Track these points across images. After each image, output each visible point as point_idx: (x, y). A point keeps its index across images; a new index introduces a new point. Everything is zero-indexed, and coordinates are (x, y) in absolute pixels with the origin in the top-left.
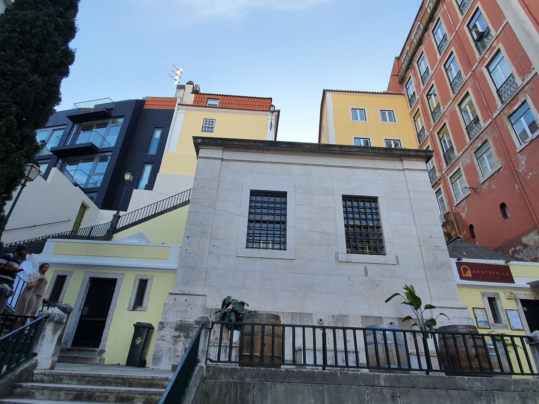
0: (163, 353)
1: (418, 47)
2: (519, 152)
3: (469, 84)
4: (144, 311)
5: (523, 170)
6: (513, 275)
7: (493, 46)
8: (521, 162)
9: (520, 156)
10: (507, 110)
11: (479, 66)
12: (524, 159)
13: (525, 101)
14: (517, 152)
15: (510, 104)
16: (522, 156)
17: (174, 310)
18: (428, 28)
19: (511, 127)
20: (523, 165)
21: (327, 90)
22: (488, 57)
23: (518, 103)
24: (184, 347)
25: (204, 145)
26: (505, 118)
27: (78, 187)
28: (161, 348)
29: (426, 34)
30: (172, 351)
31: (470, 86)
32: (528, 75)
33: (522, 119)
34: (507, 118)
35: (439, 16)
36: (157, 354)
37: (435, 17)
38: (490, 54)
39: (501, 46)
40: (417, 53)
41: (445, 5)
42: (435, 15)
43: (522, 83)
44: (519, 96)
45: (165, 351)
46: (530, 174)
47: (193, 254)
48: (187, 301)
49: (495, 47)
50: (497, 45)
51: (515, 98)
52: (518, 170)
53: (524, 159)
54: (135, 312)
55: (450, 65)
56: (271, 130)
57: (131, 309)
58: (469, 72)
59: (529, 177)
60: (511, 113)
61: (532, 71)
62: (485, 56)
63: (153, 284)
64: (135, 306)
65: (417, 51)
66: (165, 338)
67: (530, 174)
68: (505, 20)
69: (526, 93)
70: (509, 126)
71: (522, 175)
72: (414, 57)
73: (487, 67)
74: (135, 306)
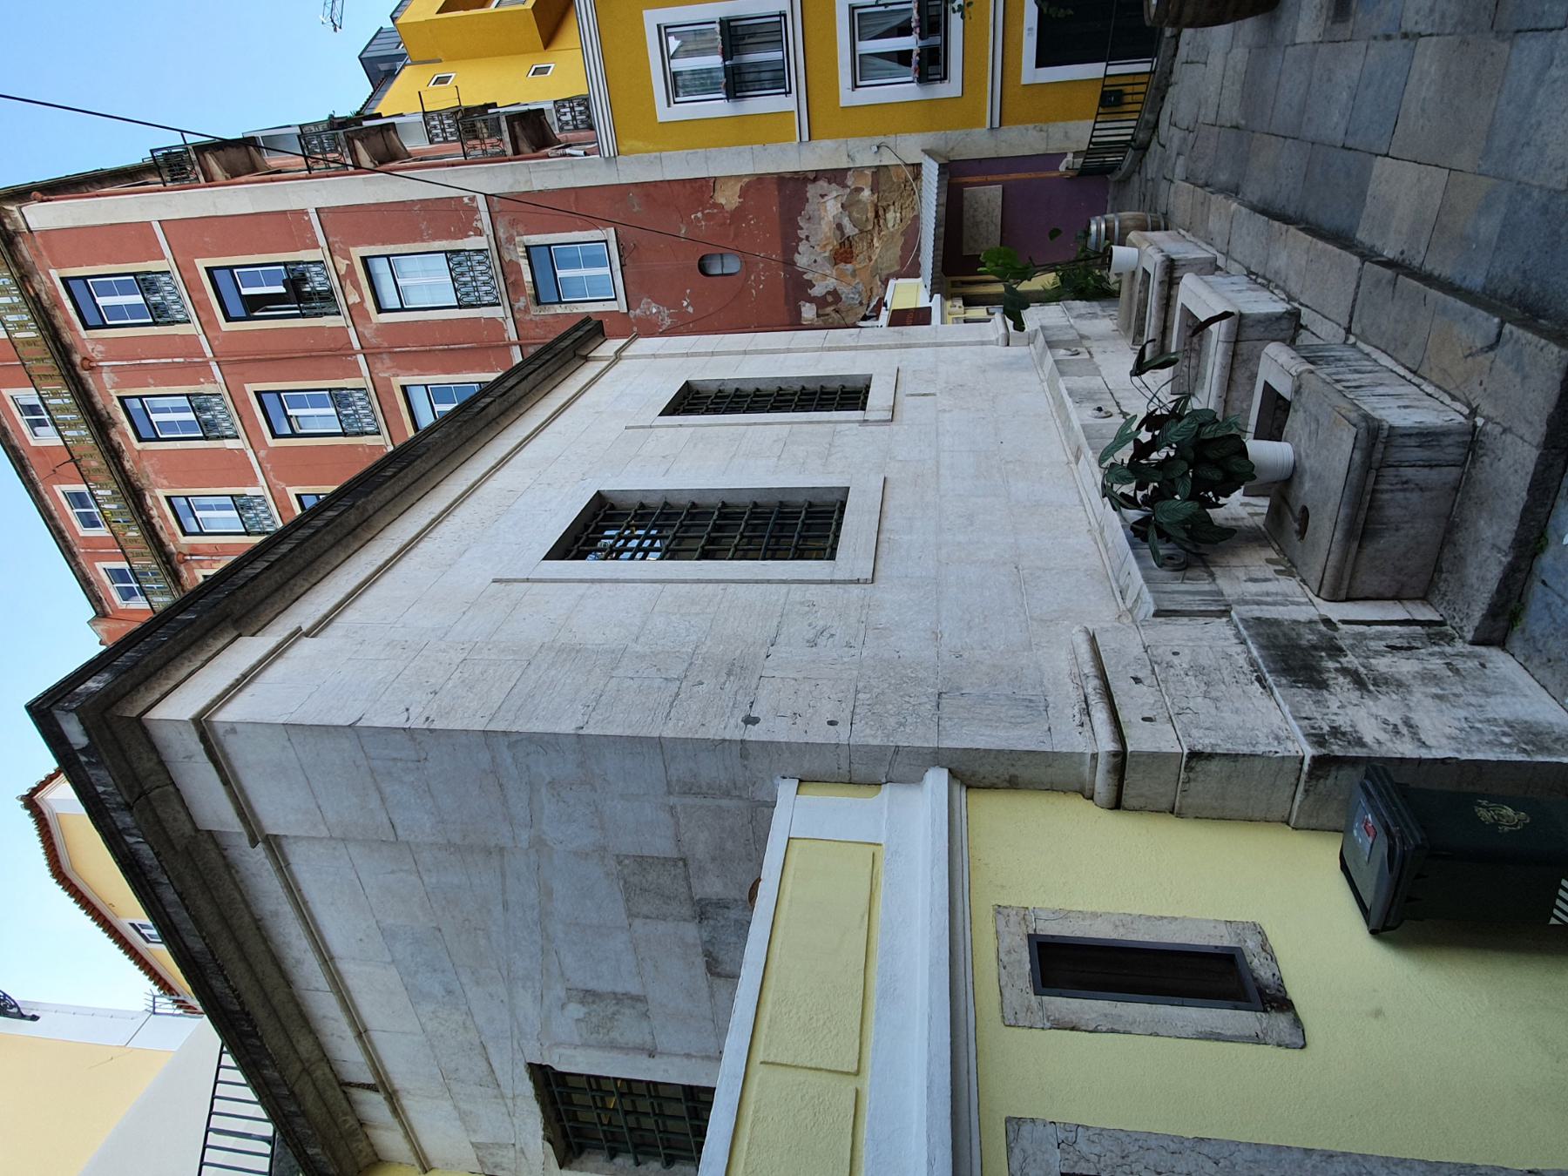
0: (1480, 722)
1: (142, 506)
2: (628, 310)
3: (386, 375)
4: (1261, 933)
5: (670, 316)
6: (913, 306)
7: (342, 272)
8: (651, 313)
9: (638, 311)
10: (518, 301)
11: (360, 329)
12: (648, 303)
13: (528, 248)
14: (626, 311)
15: (513, 286)
16: (639, 307)
17: (1213, 711)
18: (117, 446)
19: (563, 306)
20: (659, 312)
21: (35, 791)
22: (361, 296)
23: (522, 266)
24: (1386, 652)
25: (135, 687)
26: (535, 311)
27: (372, 90)
28: (1461, 730)
29: (125, 463)
30: (1443, 689)
31: (394, 376)
32: (477, 217)
33: (560, 274)
34: (538, 308)
35: (114, 393)
36: (1506, 740)
37: (104, 412)
38: (357, 286)
39: (357, 252)
40: (157, 521)
41: (101, 364)
42: (100, 406)
43: (485, 237)
44: (507, 258)
45: (1462, 713)
46: (685, 304)
47: (860, 696)
48: (1140, 675)
49: (351, 267)
50: (350, 259)
51: (508, 270)
52: (664, 328)
53: (648, 303)
54: (1294, 993)
55: (289, 418)
56: (34, 1018)
57: (1281, 1021)
58: (357, 362)
59: (690, 310)
60: (533, 292)
61: (475, 205)
62: (350, 302)
63: (1056, 903)
64: (1254, 994)
65: (150, 517)
66: (1395, 718)
67: (685, 304)
68: (307, 213)
69: (510, 240)
70: (559, 309)
71: (679, 323)
72: (157, 535)
73: (380, 310)
74: (1254, 994)
